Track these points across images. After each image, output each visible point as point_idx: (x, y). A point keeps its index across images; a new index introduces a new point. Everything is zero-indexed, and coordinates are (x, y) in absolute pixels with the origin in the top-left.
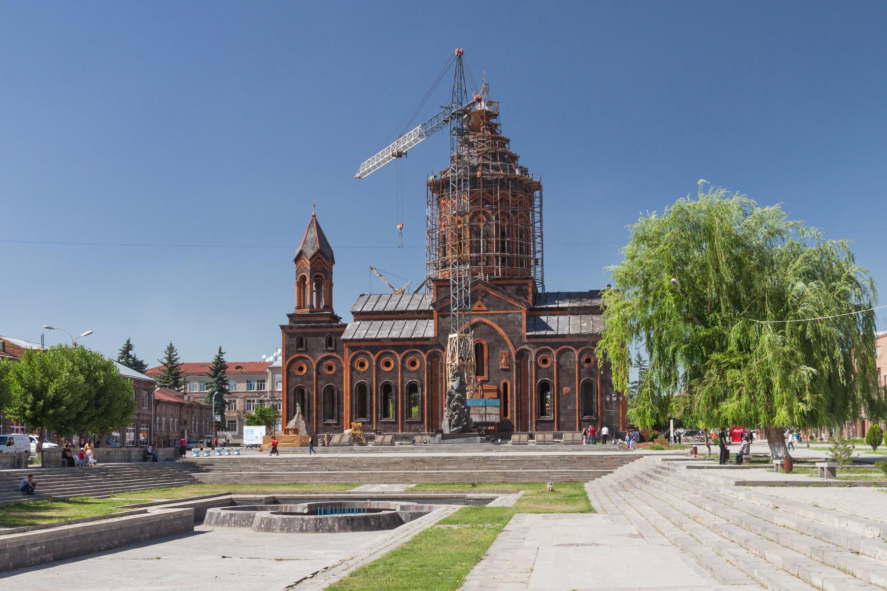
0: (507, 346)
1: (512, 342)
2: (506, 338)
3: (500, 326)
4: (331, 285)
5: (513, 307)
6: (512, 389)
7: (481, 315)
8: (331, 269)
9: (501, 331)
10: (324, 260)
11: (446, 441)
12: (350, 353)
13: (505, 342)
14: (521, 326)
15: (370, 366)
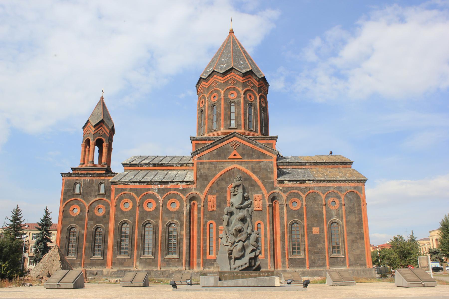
0: (260, 189)
1: (265, 186)
2: (260, 183)
3: (254, 173)
4: (110, 149)
5: (264, 156)
6: (265, 229)
7: (237, 163)
8: (112, 138)
9: (254, 177)
10: (106, 128)
11: (225, 283)
12: (116, 194)
13: (258, 186)
14: (272, 173)
15: (134, 206)
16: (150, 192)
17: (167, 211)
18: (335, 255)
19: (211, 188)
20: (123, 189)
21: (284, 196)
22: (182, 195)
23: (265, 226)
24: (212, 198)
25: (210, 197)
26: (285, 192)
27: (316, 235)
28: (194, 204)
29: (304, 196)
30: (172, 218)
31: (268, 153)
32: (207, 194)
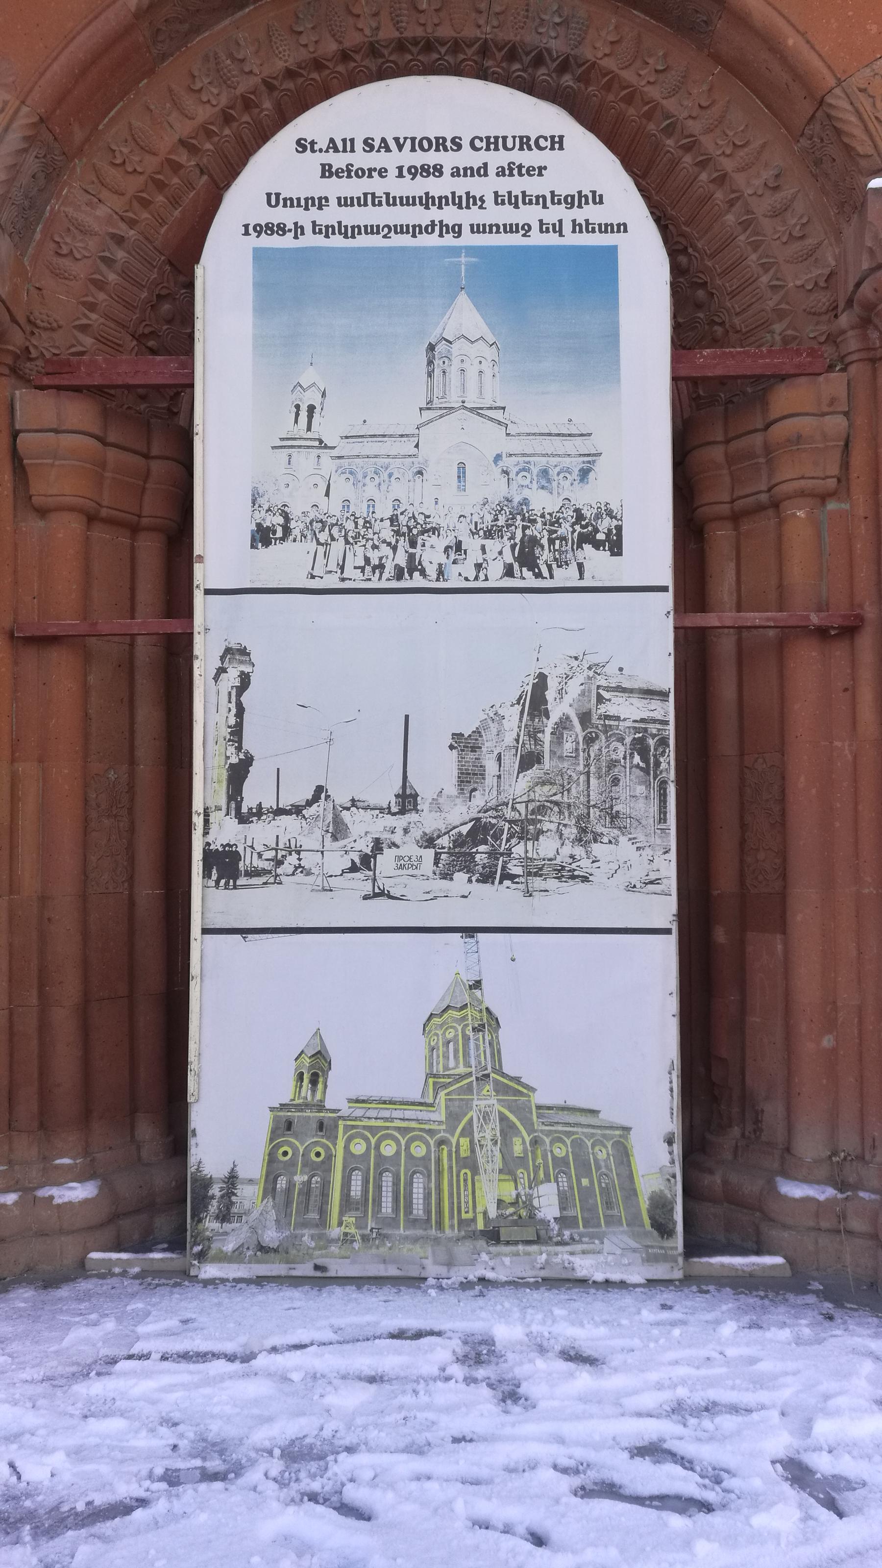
2: (518, 1124)
3: (511, 1112)
16: (389, 1132)
17: (410, 1156)
18: (609, 1212)
19: (463, 1129)
20: (353, 1127)
21: (547, 1141)
22: (428, 1138)
23: (529, 1175)
24: (465, 1142)
25: (462, 1140)
26: (547, 1136)
27: (586, 1187)
28: (443, 1149)
29: (568, 1142)
30: (417, 1166)
31: (525, 1091)
32: (459, 1137)
